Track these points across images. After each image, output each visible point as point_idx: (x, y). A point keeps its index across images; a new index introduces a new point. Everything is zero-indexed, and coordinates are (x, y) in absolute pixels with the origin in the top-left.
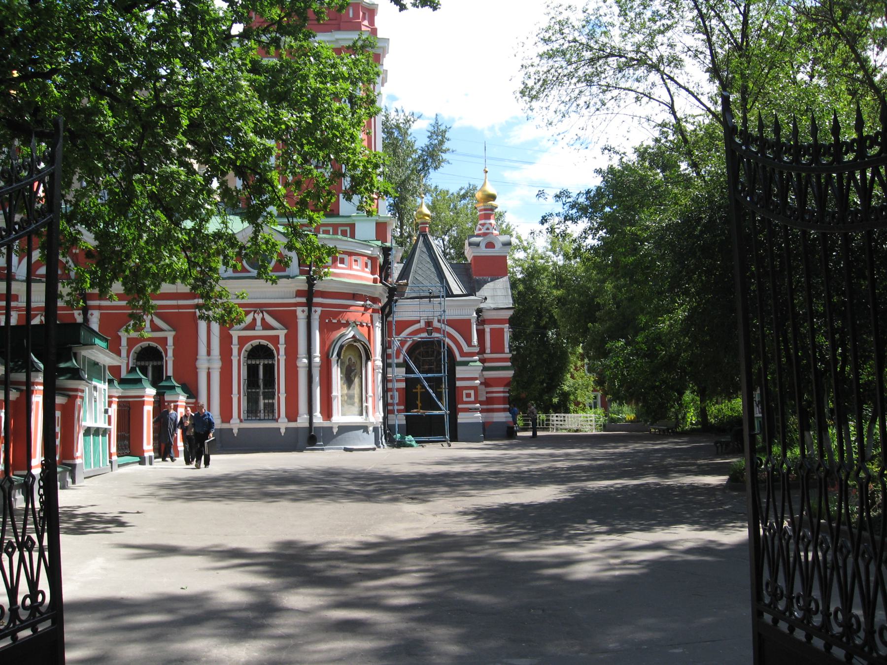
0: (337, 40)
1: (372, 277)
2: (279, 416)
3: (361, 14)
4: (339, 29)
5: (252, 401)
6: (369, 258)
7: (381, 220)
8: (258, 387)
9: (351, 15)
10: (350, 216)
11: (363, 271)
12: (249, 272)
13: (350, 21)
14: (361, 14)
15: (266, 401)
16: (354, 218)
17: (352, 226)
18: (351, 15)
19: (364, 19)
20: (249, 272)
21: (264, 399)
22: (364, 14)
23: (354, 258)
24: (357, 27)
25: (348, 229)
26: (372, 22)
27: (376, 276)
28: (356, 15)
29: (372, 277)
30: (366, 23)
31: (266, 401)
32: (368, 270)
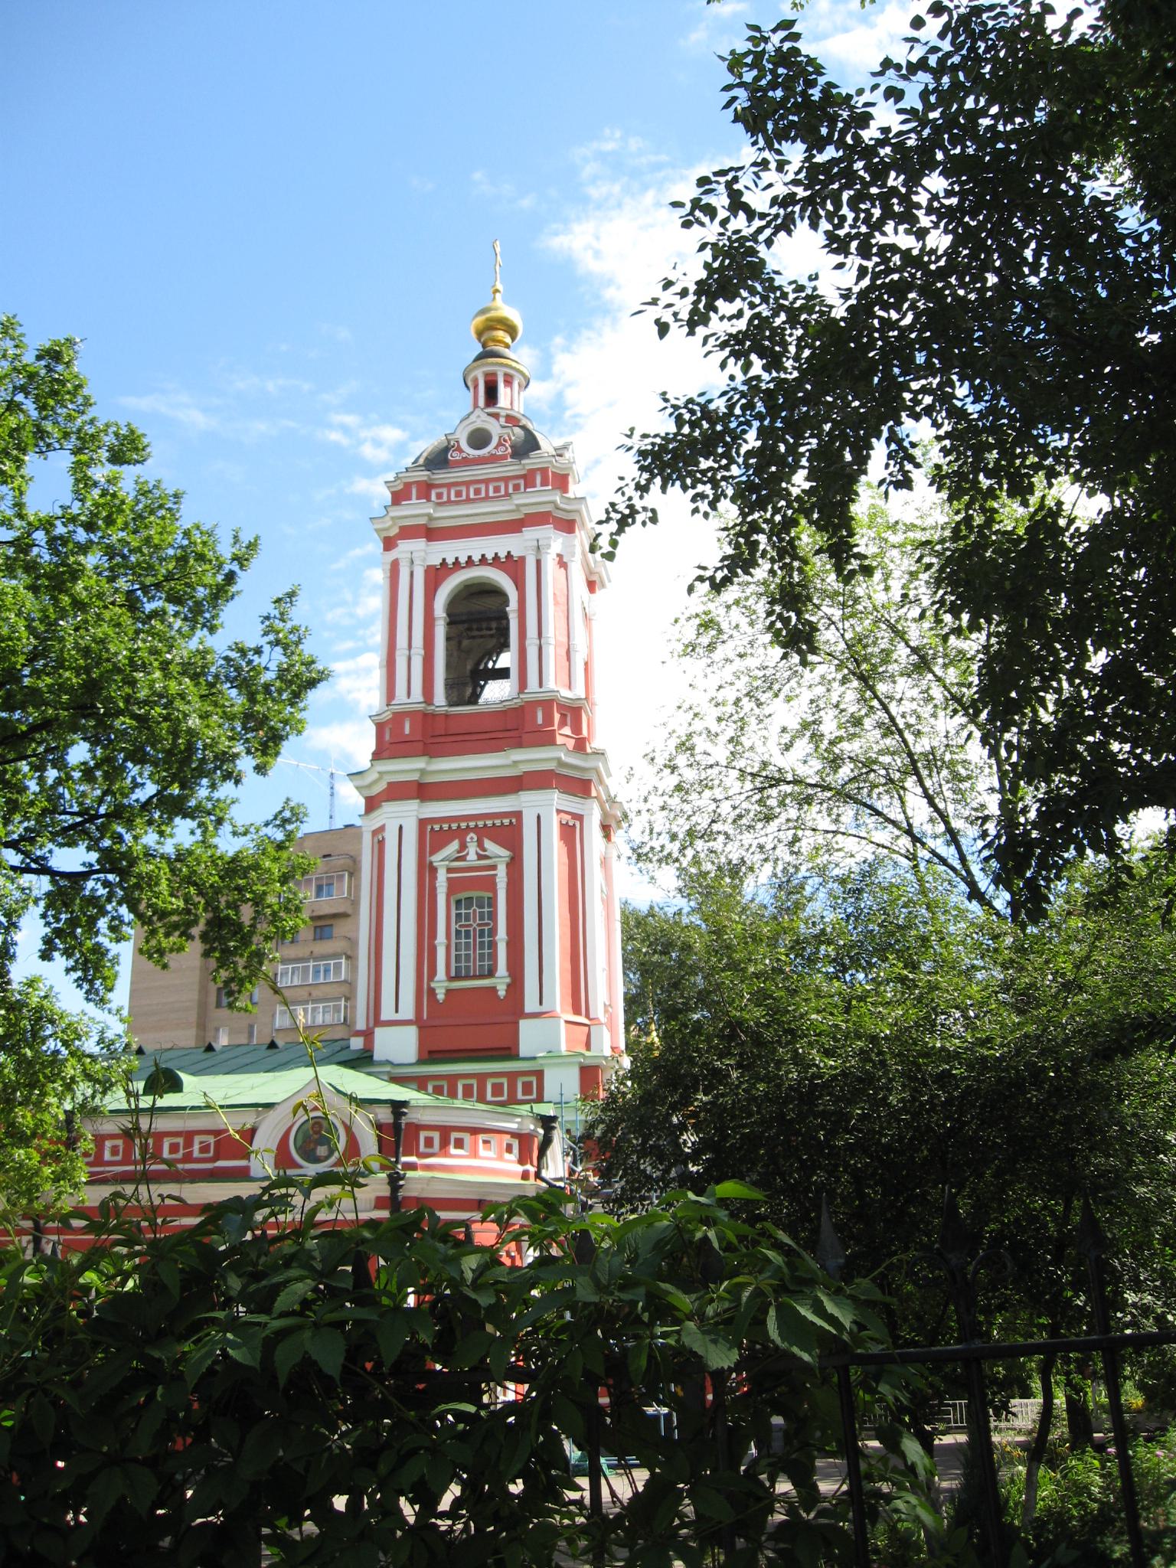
0: (515, 762)
1: (520, 1169)
3: (557, 717)
4: (519, 744)
6: (514, 1135)
7: (588, 1062)
9: (540, 721)
10: (534, 1058)
11: (500, 1158)
12: (300, 1167)
13: (538, 731)
14: (557, 717)
16: (541, 1061)
17: (539, 1074)
18: (540, 721)
19: (563, 724)
20: (300, 1167)
22: (563, 716)
23: (481, 1137)
24: (548, 740)
25: (534, 1079)
26: (577, 728)
27: (528, 1167)
28: (548, 719)
29: (520, 1169)
30: (567, 730)
32: (513, 1157)
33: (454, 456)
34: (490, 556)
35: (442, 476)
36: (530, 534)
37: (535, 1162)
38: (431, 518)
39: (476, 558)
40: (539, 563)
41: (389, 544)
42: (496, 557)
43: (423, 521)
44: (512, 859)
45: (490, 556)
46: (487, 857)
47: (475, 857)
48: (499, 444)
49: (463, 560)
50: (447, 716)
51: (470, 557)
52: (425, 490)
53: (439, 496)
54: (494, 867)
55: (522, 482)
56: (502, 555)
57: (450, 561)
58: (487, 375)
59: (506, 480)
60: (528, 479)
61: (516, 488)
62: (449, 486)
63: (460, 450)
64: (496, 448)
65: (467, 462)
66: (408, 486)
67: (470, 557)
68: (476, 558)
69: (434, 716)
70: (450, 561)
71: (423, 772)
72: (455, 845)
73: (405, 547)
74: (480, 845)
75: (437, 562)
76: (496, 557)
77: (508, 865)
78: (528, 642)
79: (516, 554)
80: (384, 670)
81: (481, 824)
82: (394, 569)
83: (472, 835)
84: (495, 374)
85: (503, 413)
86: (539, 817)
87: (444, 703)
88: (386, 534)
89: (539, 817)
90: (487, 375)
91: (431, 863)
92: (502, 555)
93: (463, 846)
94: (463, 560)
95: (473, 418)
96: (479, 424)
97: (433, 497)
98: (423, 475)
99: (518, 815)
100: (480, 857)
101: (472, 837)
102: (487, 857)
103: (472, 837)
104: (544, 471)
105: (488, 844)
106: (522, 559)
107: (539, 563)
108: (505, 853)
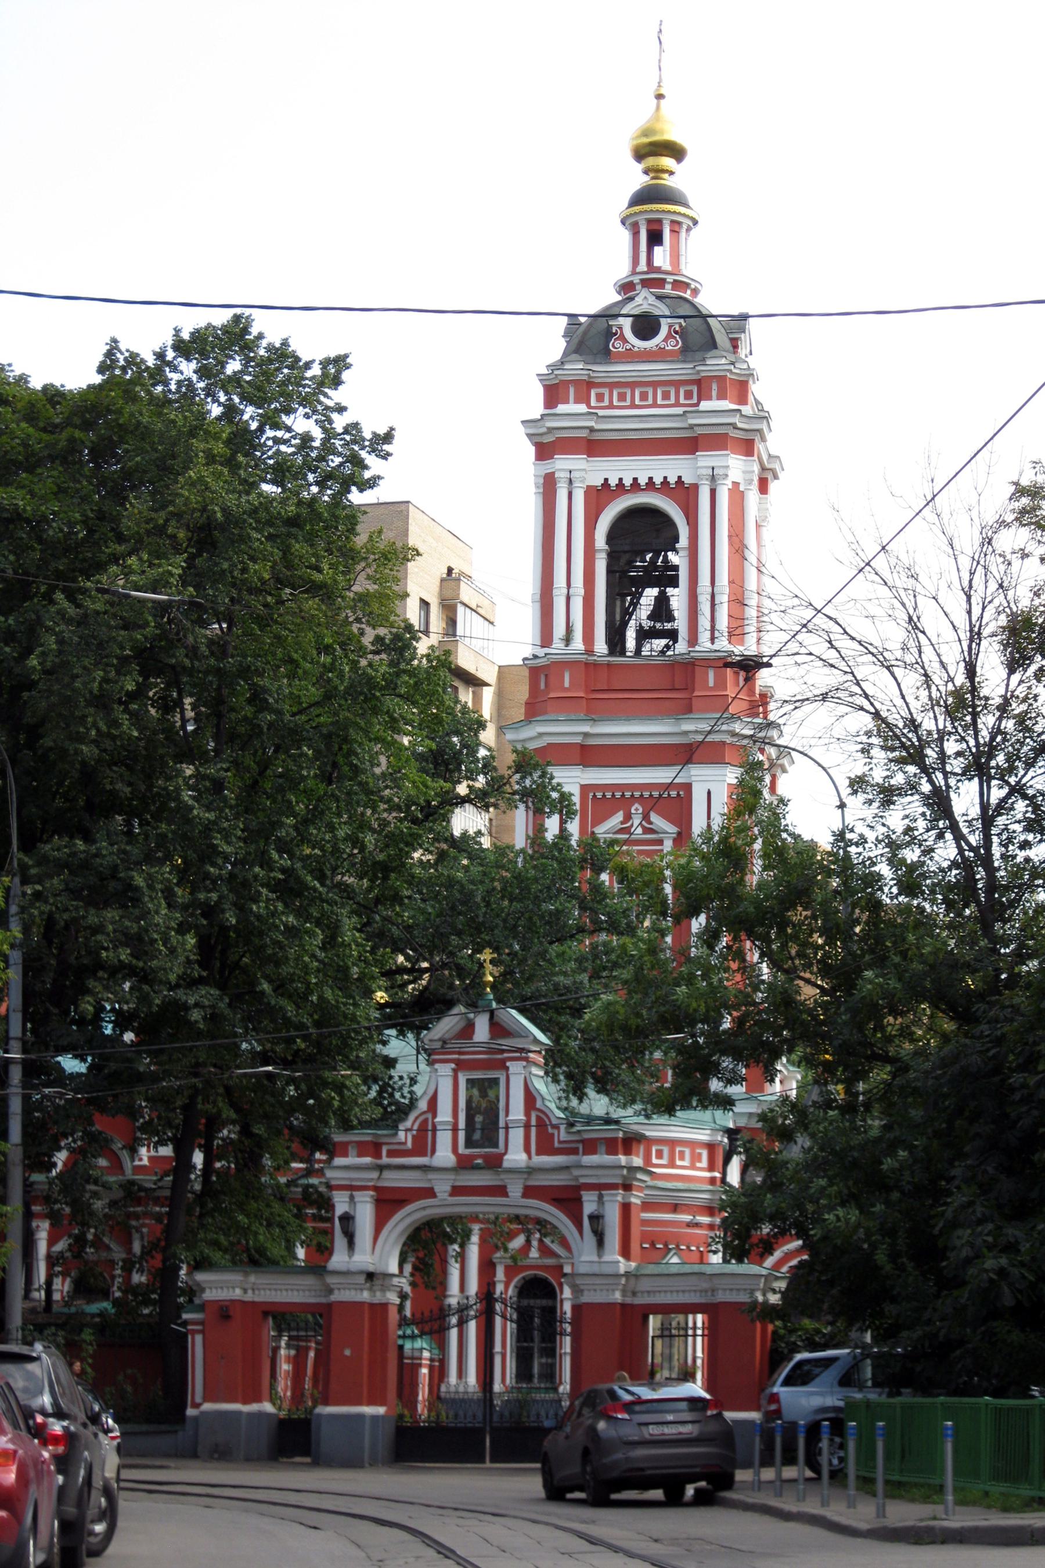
2: (561, 1383)
5: (524, 1358)
8: (532, 1340)
11: (693, 1167)
15: (544, 1360)
21: (541, 1356)
31: (544, 1360)
32: (704, 1163)
33: (616, 346)
34: (658, 480)
35: (602, 370)
36: (706, 460)
37: (721, 1170)
38: (592, 430)
39: (643, 481)
40: (713, 492)
41: (544, 451)
42: (665, 482)
43: (584, 434)
44: (679, 834)
45: (658, 480)
46: (652, 831)
47: (639, 830)
48: (669, 336)
49: (628, 482)
50: (609, 665)
51: (635, 479)
52: (584, 388)
53: (600, 397)
54: (660, 842)
55: (695, 389)
56: (672, 480)
57: (613, 482)
58: (650, 221)
59: (677, 384)
60: (702, 387)
61: (688, 395)
62: (611, 386)
63: (625, 341)
64: (665, 340)
65: (632, 356)
66: (566, 384)
67: (635, 479)
68: (643, 481)
69: (596, 665)
70: (613, 482)
71: (586, 735)
72: (619, 817)
73: (563, 464)
74: (646, 817)
75: (599, 482)
76: (665, 482)
77: (675, 840)
78: (699, 590)
79: (687, 480)
80: (538, 605)
81: (646, 794)
82: (548, 486)
83: (636, 805)
84: (659, 221)
85: (670, 279)
86: (709, 793)
87: (606, 652)
88: (538, 439)
89: (709, 793)
90: (650, 221)
91: (593, 833)
92: (672, 480)
93: (628, 817)
94: (628, 482)
95: (639, 300)
96: (645, 308)
97: (593, 403)
98: (577, 368)
99: (688, 787)
100: (646, 831)
101: (637, 809)
102: (652, 831)
103: (637, 809)
104: (721, 379)
105: (654, 817)
106: (695, 487)
107: (713, 492)
108: (672, 829)
